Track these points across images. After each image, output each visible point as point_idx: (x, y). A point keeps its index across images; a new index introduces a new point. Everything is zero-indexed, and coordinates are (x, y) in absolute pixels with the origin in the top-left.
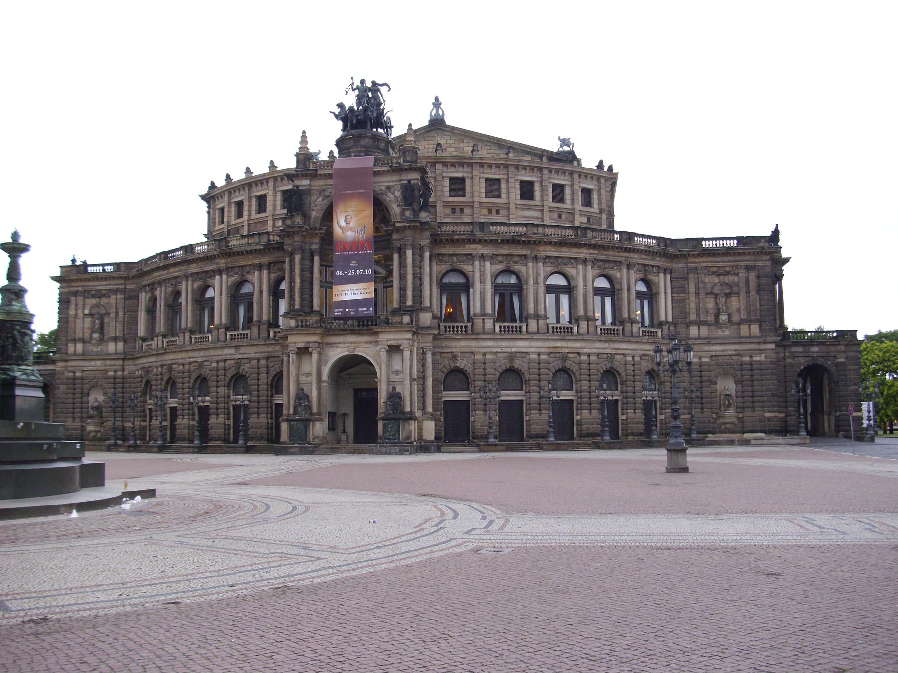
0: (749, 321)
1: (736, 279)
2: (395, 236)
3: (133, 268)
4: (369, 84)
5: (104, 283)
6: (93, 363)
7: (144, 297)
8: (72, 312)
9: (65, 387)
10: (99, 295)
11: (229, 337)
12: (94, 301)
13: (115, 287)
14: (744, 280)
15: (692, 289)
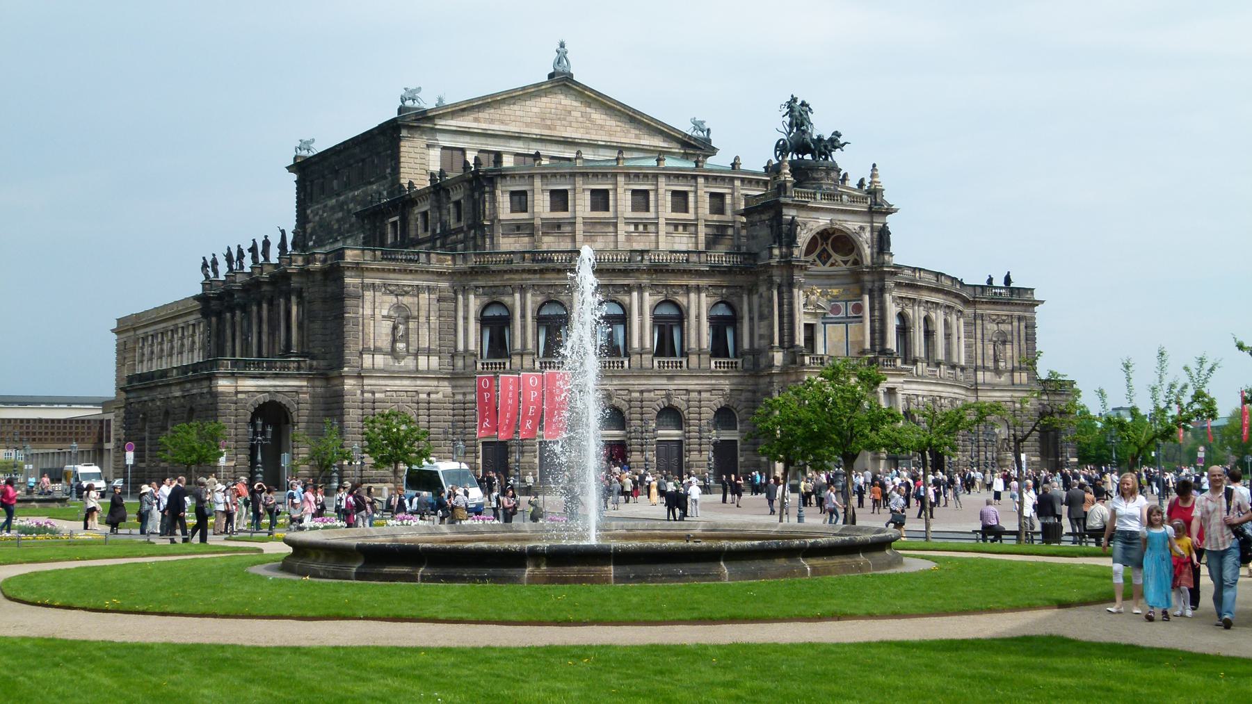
0: (1021, 369)
1: (1010, 327)
2: (867, 278)
3: (446, 260)
4: (799, 103)
5: (409, 277)
6: (398, 382)
7: (474, 303)
8: (368, 312)
9: (360, 412)
10: (401, 292)
11: (656, 364)
12: (395, 300)
13: (425, 283)
14: (1016, 329)
15: (979, 336)
